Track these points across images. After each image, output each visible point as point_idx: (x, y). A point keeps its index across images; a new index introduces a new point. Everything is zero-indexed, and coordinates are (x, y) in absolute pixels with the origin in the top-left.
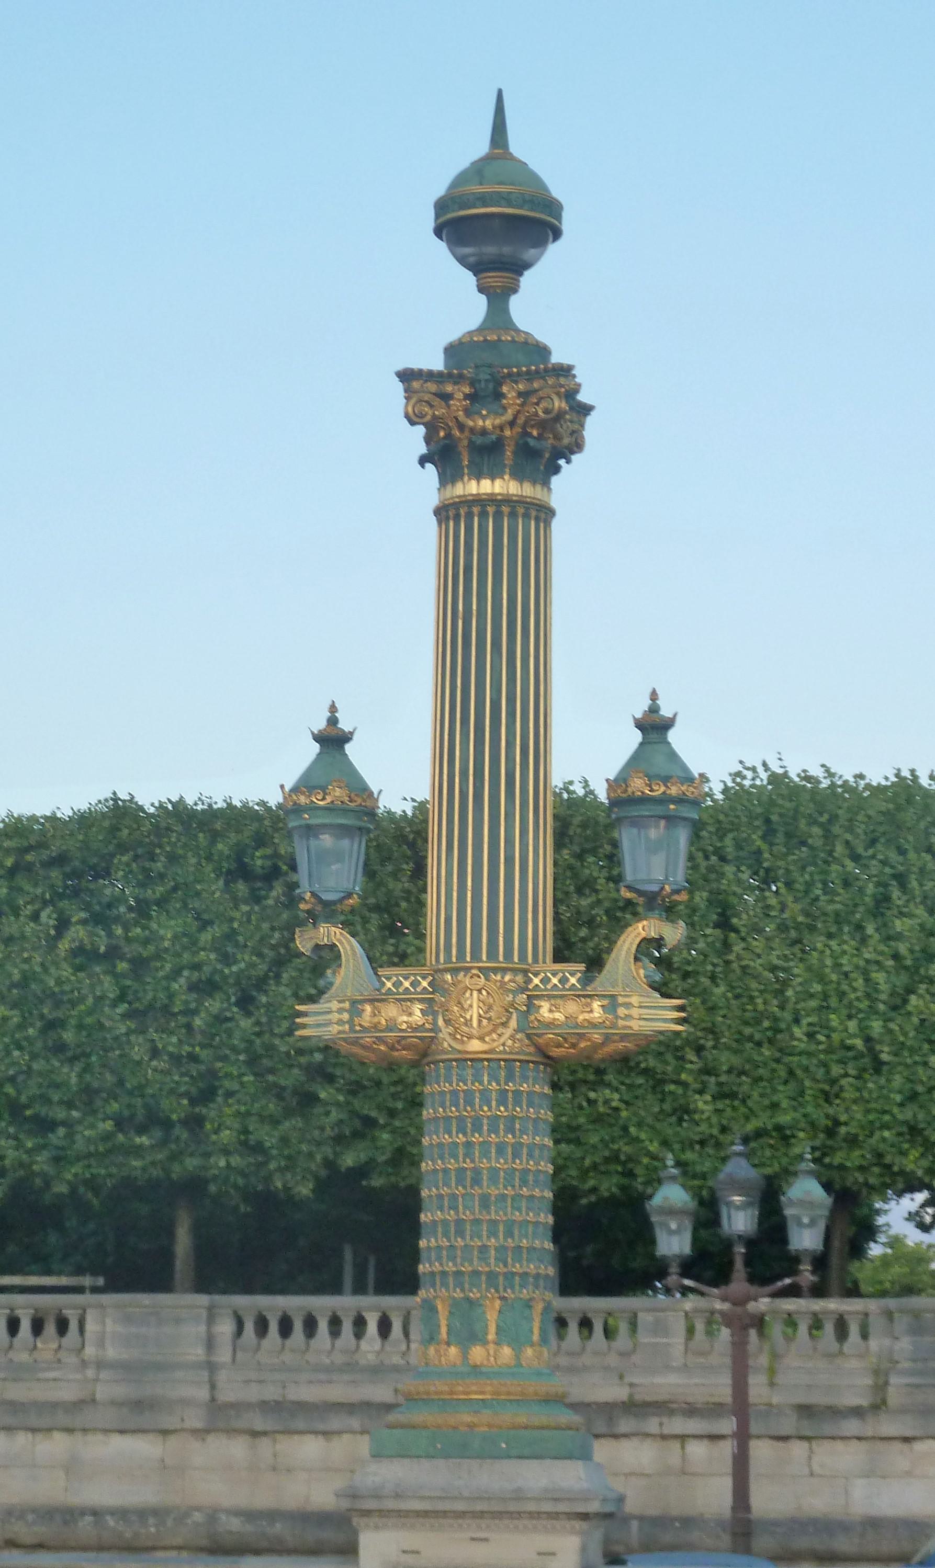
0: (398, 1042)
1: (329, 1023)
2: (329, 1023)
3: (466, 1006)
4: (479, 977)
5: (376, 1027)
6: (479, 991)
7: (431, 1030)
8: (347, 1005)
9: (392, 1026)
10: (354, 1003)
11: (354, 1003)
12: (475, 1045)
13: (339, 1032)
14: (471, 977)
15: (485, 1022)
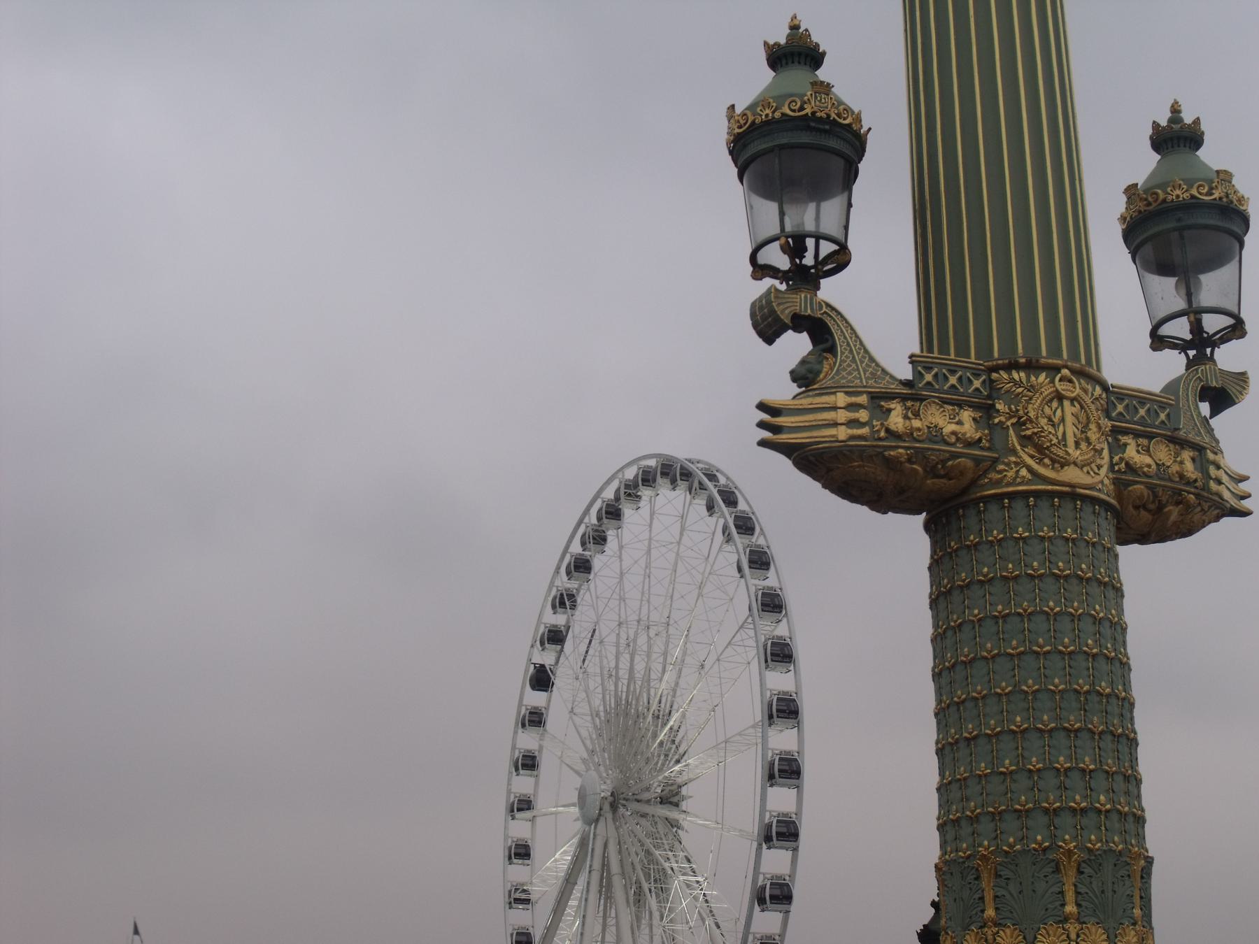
0: (944, 462)
1: (835, 424)
2: (835, 424)
3: (1056, 420)
4: (1070, 381)
5: (910, 434)
6: (1072, 400)
7: (989, 449)
8: (863, 399)
9: (935, 434)
10: (875, 397)
11: (875, 397)
12: (1071, 475)
13: (852, 438)
14: (1061, 380)
15: (1083, 445)
